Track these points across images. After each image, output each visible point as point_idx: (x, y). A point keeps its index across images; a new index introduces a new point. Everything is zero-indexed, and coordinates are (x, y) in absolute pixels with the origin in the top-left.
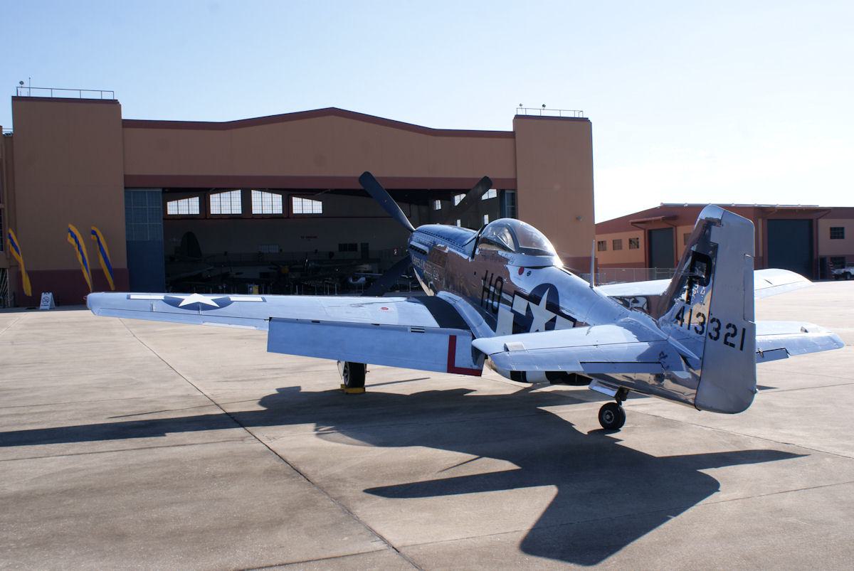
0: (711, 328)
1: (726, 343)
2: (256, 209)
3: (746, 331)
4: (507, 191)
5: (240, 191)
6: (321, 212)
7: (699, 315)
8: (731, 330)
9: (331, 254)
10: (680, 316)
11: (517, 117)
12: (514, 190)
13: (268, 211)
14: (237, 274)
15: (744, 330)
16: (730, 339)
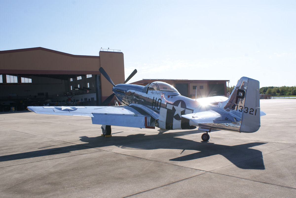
0: (245, 110)
1: (250, 113)
2: (8, 81)
3: (257, 110)
4: (97, 75)
5: (2, 75)
6: (31, 82)
7: (240, 106)
8: (252, 110)
9: (35, 96)
10: (234, 107)
11: (100, 52)
12: (100, 75)
13: (12, 82)
14: (3, 104)
15: (256, 110)
16: (251, 113)
